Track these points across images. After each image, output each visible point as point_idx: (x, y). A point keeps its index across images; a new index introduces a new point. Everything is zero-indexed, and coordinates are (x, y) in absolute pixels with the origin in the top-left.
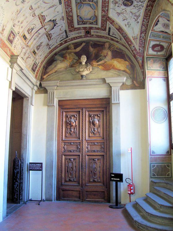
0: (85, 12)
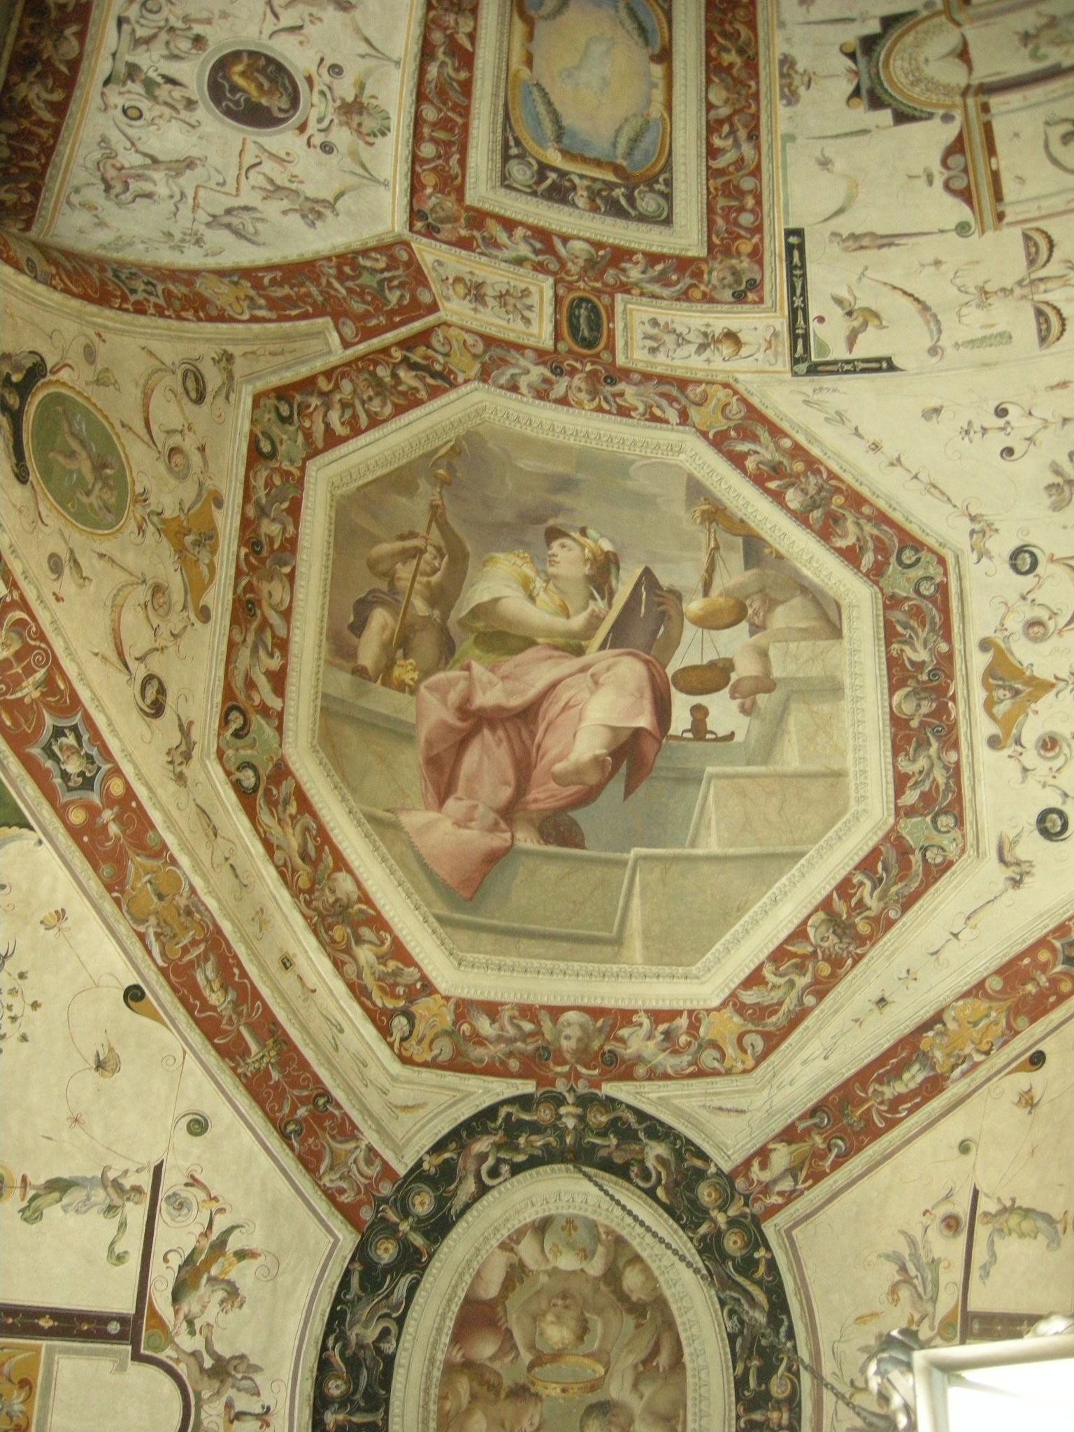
0: (605, 82)
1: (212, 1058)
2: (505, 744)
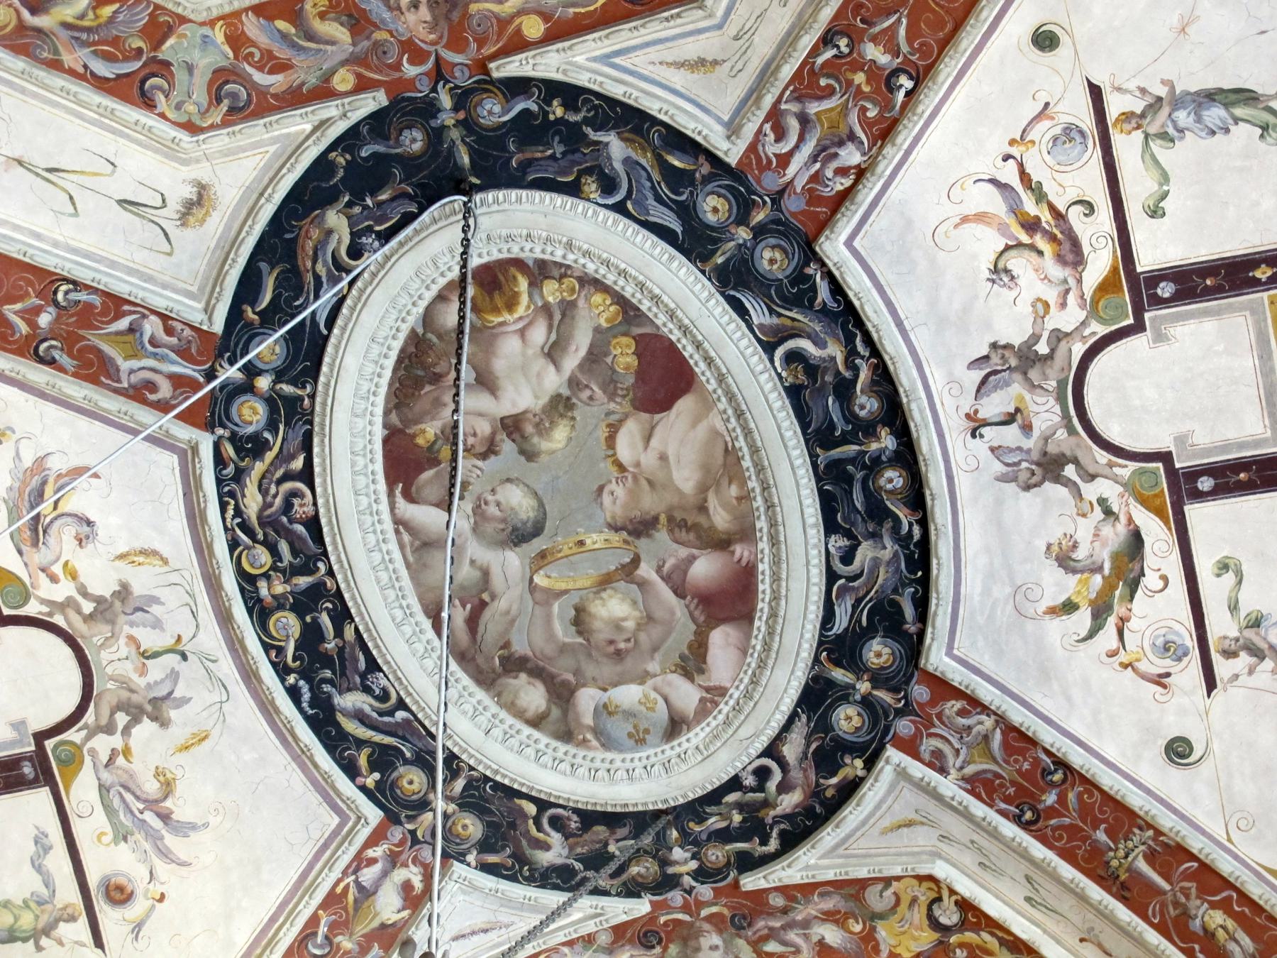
1: (1195, 844)
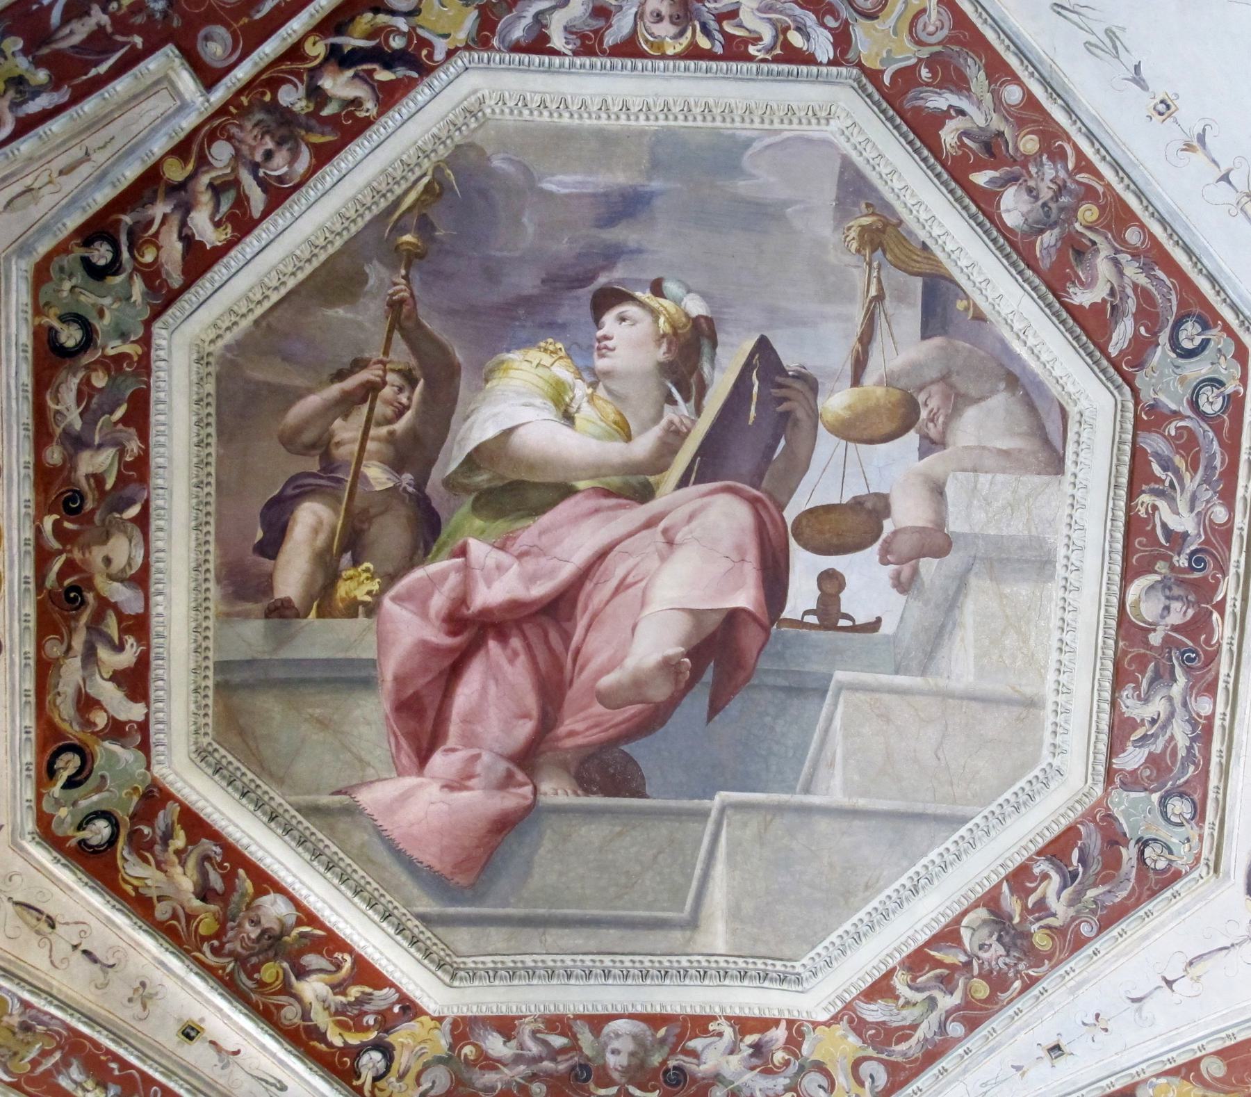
2: (522, 658)
